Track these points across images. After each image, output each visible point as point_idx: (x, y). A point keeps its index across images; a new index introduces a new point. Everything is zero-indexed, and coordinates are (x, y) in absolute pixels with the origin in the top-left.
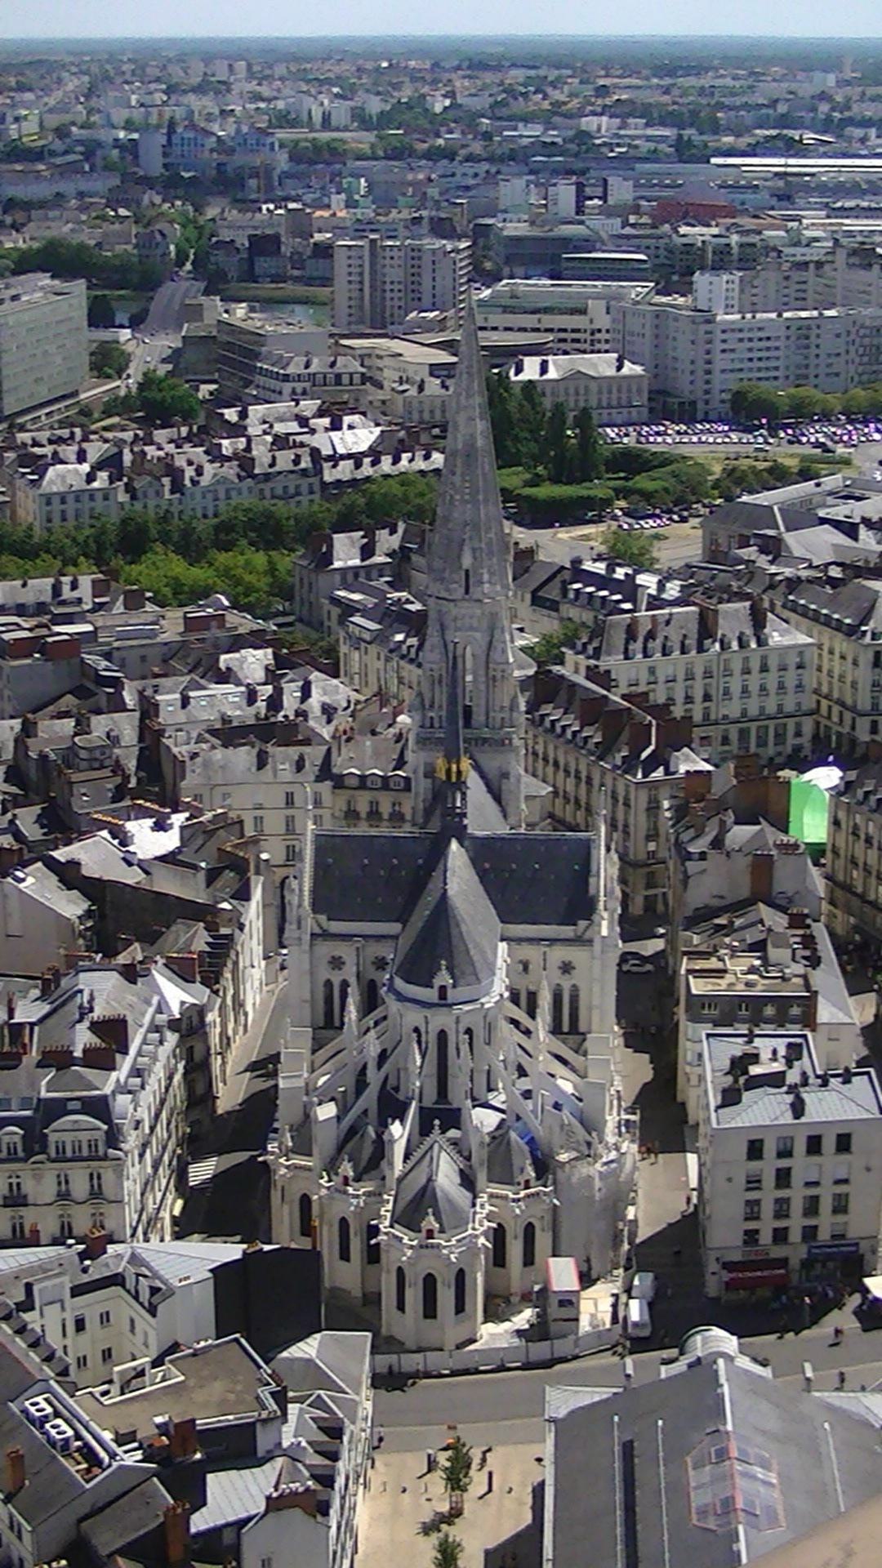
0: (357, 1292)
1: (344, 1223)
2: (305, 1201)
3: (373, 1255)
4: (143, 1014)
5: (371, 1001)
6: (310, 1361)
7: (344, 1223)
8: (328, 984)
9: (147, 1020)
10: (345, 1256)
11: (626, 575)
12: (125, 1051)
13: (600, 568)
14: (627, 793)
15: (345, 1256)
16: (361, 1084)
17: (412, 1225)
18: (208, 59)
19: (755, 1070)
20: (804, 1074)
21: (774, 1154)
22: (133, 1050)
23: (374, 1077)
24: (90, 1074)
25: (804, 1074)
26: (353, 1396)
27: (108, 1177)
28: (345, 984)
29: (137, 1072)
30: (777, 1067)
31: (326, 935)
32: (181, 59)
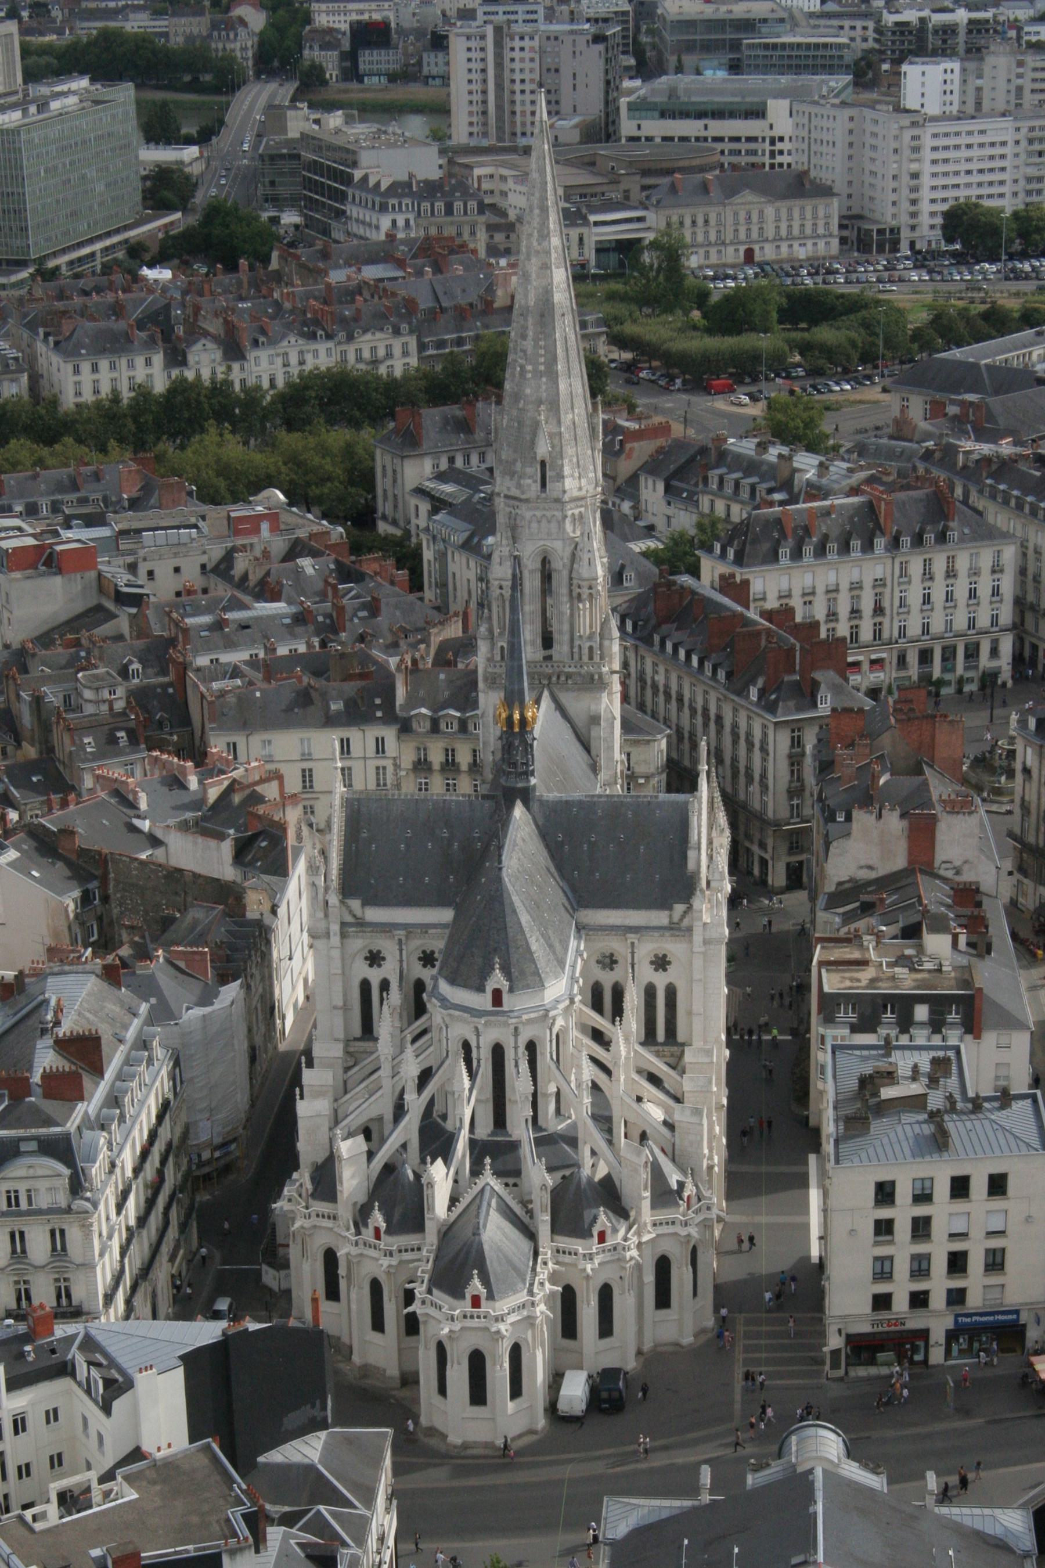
4: (126, 1027)
9: (130, 1034)
11: (780, 456)
12: (98, 1071)
13: (747, 447)
14: (765, 735)
17: (456, 1291)
19: (888, 1093)
20: (950, 1098)
21: (909, 1199)
22: (110, 1074)
24: (50, 1107)
25: (950, 1098)
27: (74, 1234)
29: (114, 1100)
30: (915, 1089)
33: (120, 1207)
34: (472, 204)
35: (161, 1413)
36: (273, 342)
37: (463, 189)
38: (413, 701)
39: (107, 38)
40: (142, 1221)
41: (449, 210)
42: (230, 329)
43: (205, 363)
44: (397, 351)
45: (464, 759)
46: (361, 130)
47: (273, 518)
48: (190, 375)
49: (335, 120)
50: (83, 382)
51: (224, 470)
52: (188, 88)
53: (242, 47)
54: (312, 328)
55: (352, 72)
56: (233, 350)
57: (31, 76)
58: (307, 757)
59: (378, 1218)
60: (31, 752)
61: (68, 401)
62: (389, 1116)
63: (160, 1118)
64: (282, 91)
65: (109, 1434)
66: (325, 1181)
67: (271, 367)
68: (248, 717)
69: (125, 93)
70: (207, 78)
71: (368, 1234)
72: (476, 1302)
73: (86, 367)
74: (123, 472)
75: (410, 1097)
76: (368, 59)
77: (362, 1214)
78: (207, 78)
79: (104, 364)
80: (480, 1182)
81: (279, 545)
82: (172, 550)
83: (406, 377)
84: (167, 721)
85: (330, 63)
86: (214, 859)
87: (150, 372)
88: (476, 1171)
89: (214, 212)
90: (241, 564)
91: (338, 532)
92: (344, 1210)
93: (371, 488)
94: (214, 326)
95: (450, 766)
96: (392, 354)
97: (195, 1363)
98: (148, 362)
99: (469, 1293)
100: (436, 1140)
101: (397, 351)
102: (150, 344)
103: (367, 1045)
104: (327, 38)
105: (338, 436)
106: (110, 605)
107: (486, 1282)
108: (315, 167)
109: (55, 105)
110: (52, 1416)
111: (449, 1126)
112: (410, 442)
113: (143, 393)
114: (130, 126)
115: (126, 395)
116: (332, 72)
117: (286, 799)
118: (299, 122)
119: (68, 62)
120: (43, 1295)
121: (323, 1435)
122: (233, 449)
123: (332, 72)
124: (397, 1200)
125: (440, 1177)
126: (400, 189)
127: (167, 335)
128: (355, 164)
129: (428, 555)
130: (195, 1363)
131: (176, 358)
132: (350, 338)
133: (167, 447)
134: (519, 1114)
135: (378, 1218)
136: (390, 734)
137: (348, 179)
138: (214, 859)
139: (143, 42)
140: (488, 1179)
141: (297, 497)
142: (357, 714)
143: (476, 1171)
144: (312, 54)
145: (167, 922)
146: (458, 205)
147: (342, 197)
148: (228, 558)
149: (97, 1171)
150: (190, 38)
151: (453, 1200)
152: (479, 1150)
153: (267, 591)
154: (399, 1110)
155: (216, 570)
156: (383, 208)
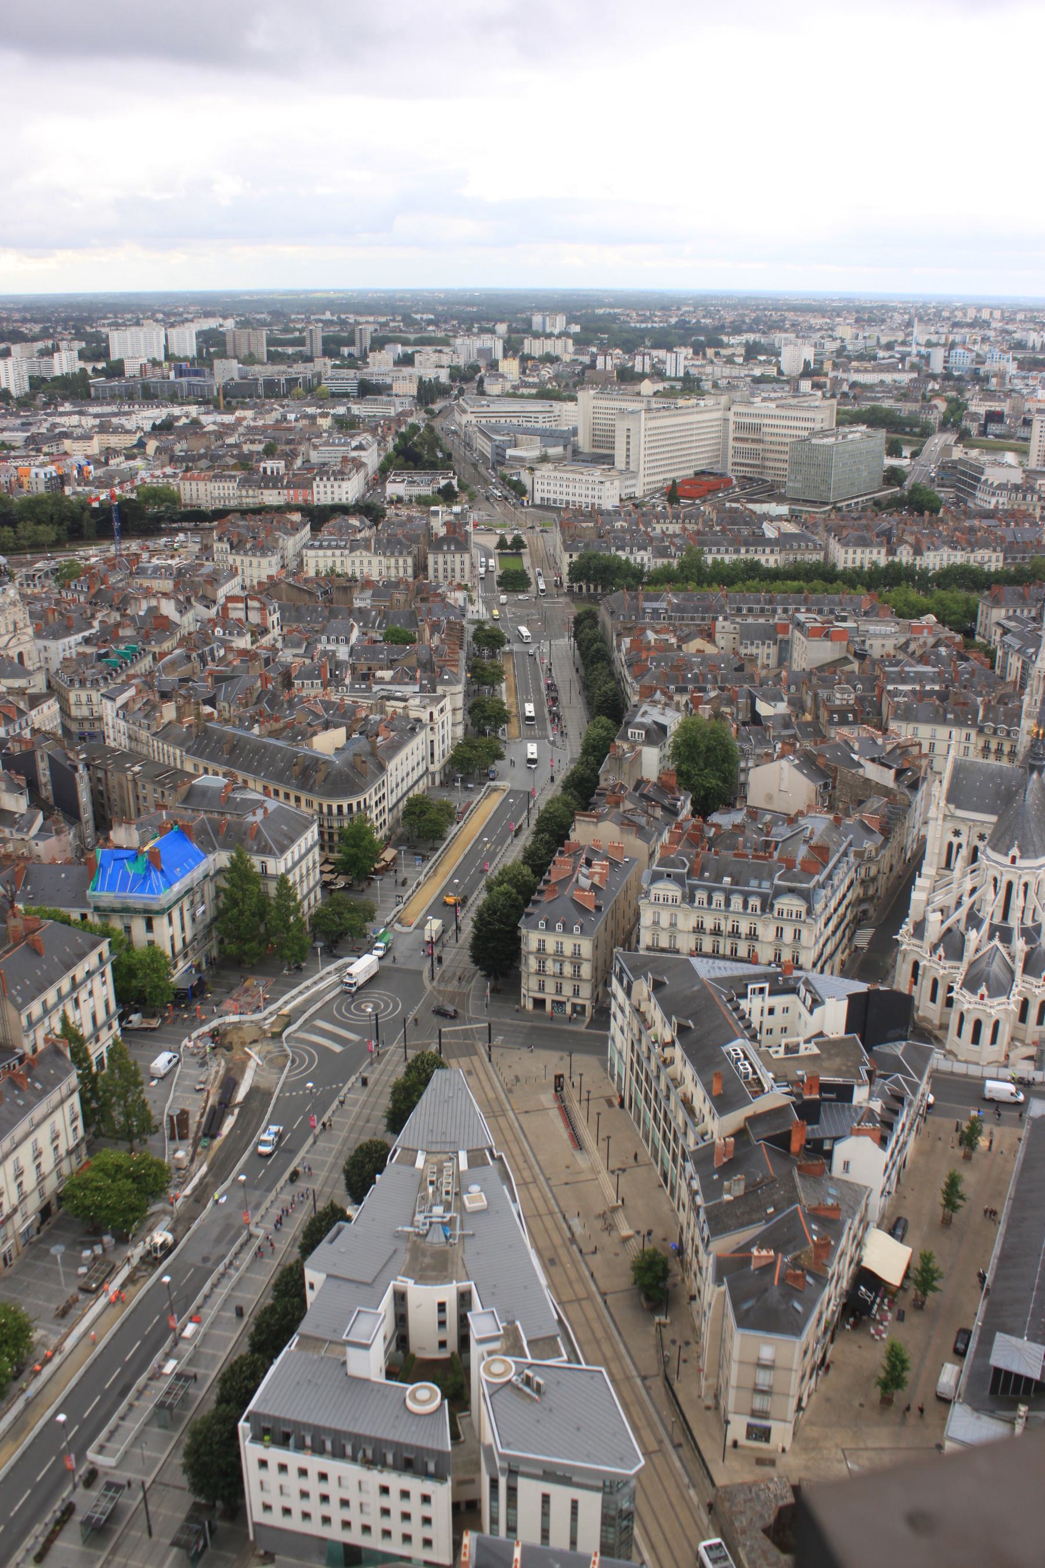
0: (937, 1022)
1: (935, 983)
2: (916, 965)
3: (949, 1002)
5: (974, 858)
6: (896, 1057)
7: (935, 983)
8: (950, 845)
10: (933, 999)
15: (933, 999)
16: (959, 904)
18: (979, 309)
23: (967, 901)
26: (917, 1080)
28: (960, 846)
29: (830, 877)
31: (953, 816)
32: (964, 309)
33: (826, 925)
34: (1036, 497)
35: (833, 1017)
36: (936, 549)
37: (1032, 489)
38: (985, 718)
39: (874, 410)
40: (834, 933)
41: (1024, 498)
42: (918, 541)
43: (904, 556)
44: (994, 559)
45: (1006, 748)
46: (986, 458)
47: (930, 628)
48: (897, 560)
49: (974, 453)
50: (847, 557)
51: (907, 603)
52: (906, 434)
53: (934, 418)
54: (954, 545)
55: (984, 432)
56: (918, 552)
57: (840, 423)
58: (933, 737)
59: (941, 951)
60: (808, 717)
61: (840, 567)
62: (953, 905)
63: (849, 888)
64: (950, 438)
65: (813, 1023)
66: (919, 930)
67: (935, 560)
68: (907, 715)
69: (882, 434)
70: (917, 430)
71: (935, 958)
72: (982, 997)
73: (851, 551)
74: (864, 598)
75: (965, 898)
76: (993, 428)
77: (934, 948)
78: (917, 430)
79: (859, 551)
80: (993, 943)
81: (931, 641)
82: (883, 636)
83: (996, 571)
84: (869, 712)
85: (974, 428)
86: (886, 777)
87: (879, 557)
88: (991, 937)
89: (915, 489)
90: (913, 646)
91: (959, 638)
92: (927, 944)
93: (975, 620)
94: (911, 539)
95: (999, 752)
96: (991, 560)
97: (853, 999)
98: (879, 553)
99: (980, 992)
100: (974, 920)
101: (994, 559)
102: (880, 545)
103: (947, 872)
104: (974, 417)
105: (962, 594)
106: (851, 658)
107: (988, 989)
108: (964, 473)
109: (850, 436)
110: (786, 1010)
111: (981, 915)
112: (997, 602)
113: (874, 563)
114: (883, 447)
115: (867, 566)
116: (974, 432)
117: (922, 756)
118: (958, 453)
119: (856, 419)
120: (786, 956)
121: (904, 1043)
122: (914, 596)
123: (974, 432)
124: (952, 944)
125: (973, 937)
126: (1002, 487)
127: (889, 542)
128: (982, 473)
129: (999, 653)
130: (853, 999)
131: (892, 552)
132: (973, 551)
133: (884, 590)
134: (1015, 915)
135: (941, 951)
136: (973, 733)
137: (978, 480)
138: (886, 777)
139: (890, 412)
140: (996, 942)
141: (942, 621)
142: (959, 722)
143: (991, 937)
144: (966, 423)
145: (861, 802)
146: (1029, 497)
147: (974, 488)
148: (907, 644)
149: (818, 907)
150: (911, 412)
151: (977, 951)
152: (993, 929)
153: (923, 660)
154: (959, 904)
155: (900, 648)
156: (993, 494)
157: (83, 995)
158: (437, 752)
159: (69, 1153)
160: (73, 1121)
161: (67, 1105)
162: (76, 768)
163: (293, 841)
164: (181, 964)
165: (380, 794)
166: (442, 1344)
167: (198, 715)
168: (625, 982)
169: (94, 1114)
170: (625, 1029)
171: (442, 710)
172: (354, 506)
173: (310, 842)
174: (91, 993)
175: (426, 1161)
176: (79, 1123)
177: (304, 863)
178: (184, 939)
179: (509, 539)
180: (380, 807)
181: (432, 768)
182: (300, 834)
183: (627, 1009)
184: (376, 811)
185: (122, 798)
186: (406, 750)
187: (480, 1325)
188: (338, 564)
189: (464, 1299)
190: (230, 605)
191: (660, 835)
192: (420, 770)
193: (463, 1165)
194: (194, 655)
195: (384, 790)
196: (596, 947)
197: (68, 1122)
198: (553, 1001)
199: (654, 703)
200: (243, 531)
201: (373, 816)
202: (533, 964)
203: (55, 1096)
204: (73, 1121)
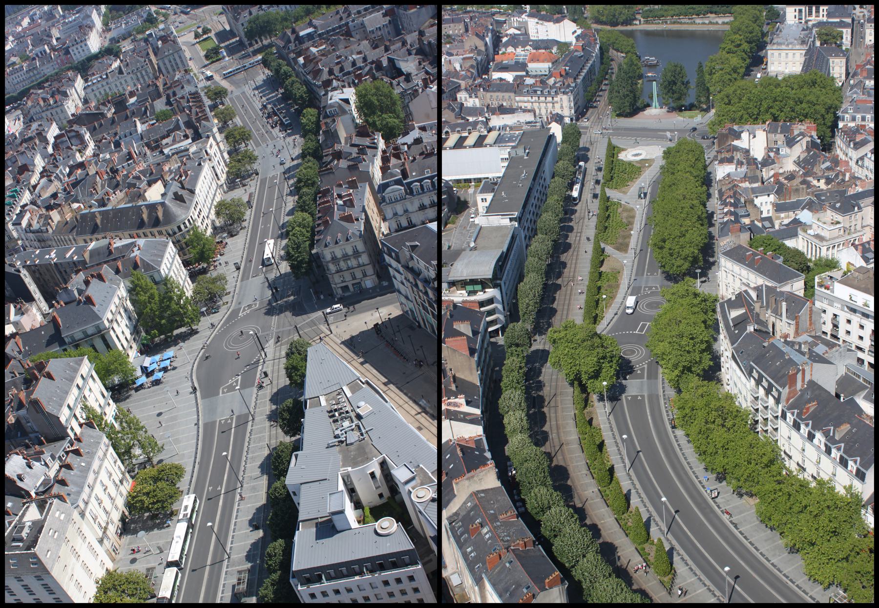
157: (87, 393)
158: (219, 172)
159: (121, 482)
160: (115, 462)
161: (108, 455)
162: (19, 271)
163: (162, 257)
164: (130, 354)
165: (198, 210)
166: (381, 496)
167: (72, 210)
168: (393, 254)
169: (124, 454)
170: (405, 281)
171: (211, 146)
172: (100, 52)
173: (172, 254)
174: (90, 389)
175: (327, 400)
176: (119, 462)
177: (174, 267)
178: (126, 338)
179: (200, 31)
180: (201, 217)
181: (220, 183)
182: (164, 251)
183: (401, 270)
184: (200, 220)
185: (52, 277)
186: (201, 178)
187: (401, 474)
188: (108, 90)
189: (383, 464)
190: (58, 141)
191: (373, 164)
192: (214, 186)
193: (349, 394)
194: (53, 178)
195: (199, 207)
196: (365, 243)
197: (113, 464)
198: (353, 285)
199: (335, 89)
200: (44, 95)
201: (200, 224)
202: (332, 268)
203: (100, 453)
204: (115, 462)
